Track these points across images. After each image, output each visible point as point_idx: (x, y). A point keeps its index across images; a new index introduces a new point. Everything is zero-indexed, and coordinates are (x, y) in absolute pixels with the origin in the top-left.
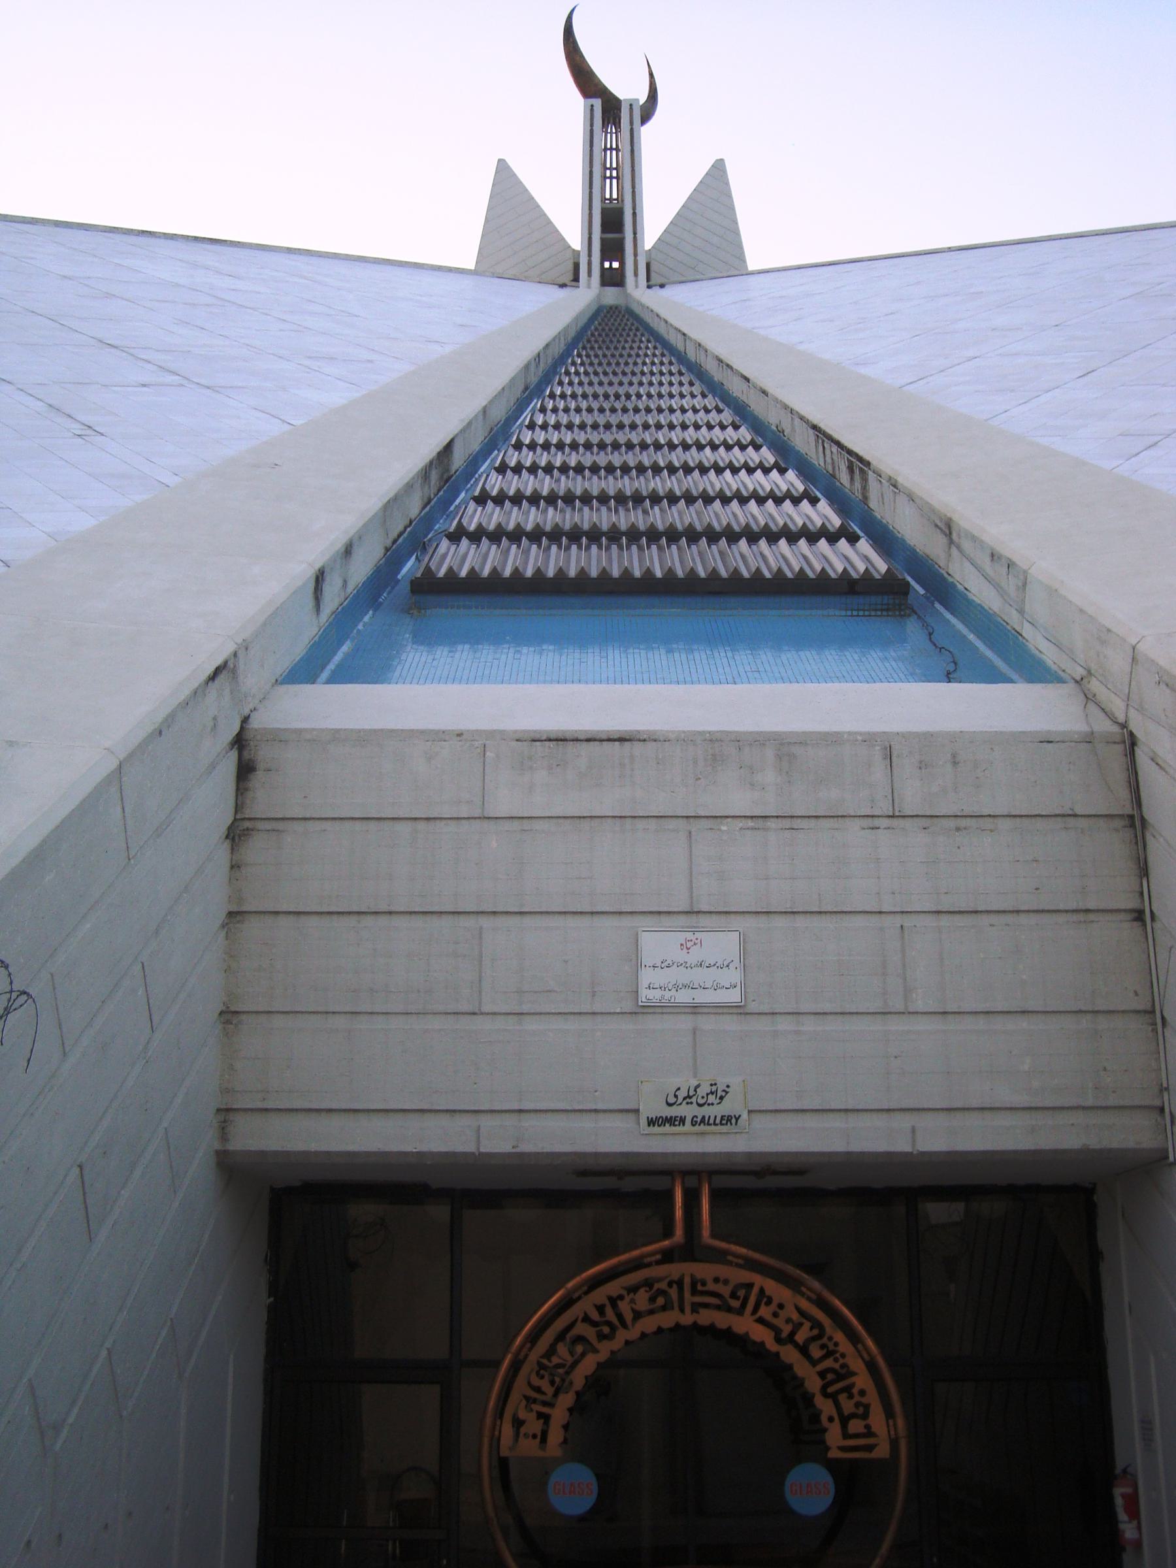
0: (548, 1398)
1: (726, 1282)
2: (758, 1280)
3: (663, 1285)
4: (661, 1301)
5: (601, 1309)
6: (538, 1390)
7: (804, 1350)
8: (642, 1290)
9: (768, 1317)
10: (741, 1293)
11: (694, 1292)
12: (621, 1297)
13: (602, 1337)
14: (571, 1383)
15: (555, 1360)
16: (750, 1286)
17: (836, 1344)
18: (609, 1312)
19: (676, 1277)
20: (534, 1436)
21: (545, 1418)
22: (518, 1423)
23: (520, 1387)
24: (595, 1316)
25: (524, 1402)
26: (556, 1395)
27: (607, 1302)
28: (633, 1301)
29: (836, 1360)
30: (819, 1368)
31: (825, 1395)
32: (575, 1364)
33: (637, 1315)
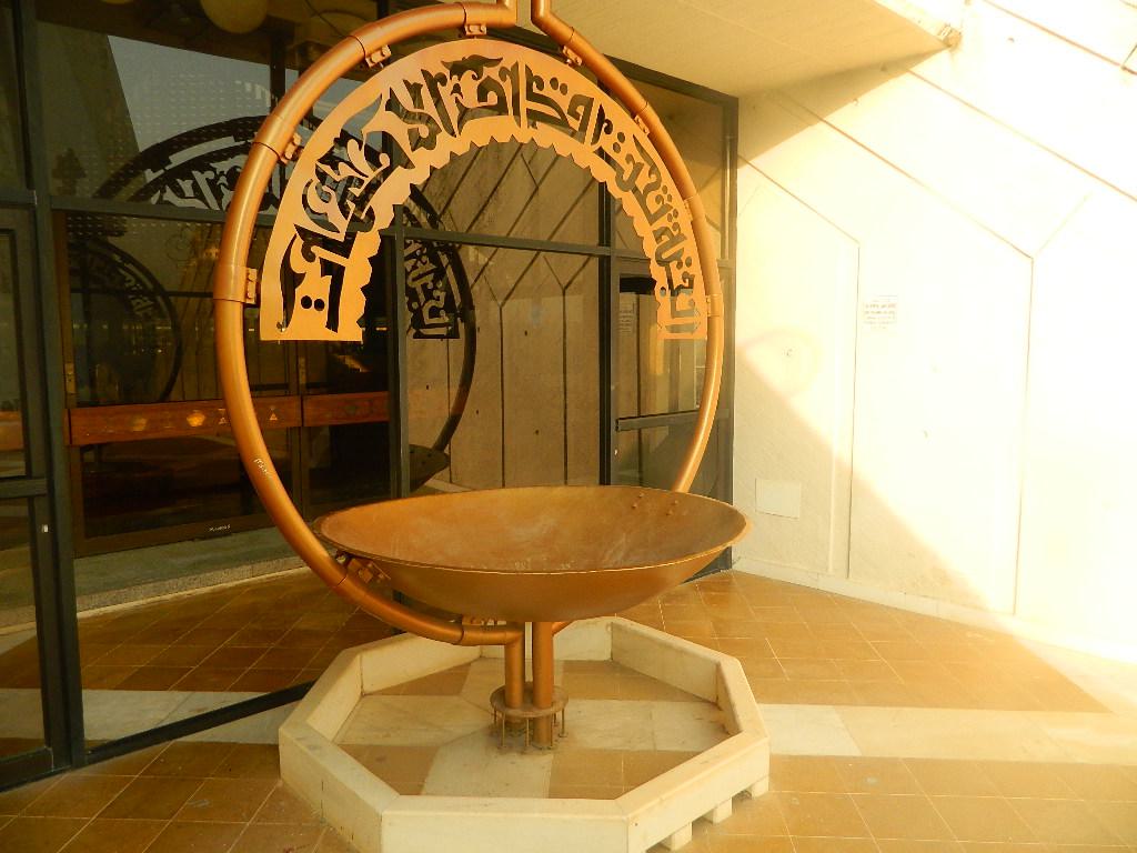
0: (340, 237)
1: (564, 89)
2: (601, 99)
3: (491, 72)
4: (492, 98)
5: (414, 89)
6: (321, 220)
7: (642, 200)
8: (468, 74)
9: (609, 150)
10: (581, 110)
11: (531, 96)
12: (443, 80)
13: (417, 142)
14: (371, 214)
15: (345, 171)
16: (589, 103)
17: (670, 198)
18: (425, 93)
19: (508, 64)
20: (319, 305)
21: (335, 273)
22: (290, 280)
23: (290, 217)
24: (405, 99)
25: (299, 242)
26: (351, 237)
27: (422, 81)
28: (457, 89)
29: (670, 219)
30: (658, 225)
31: (661, 262)
32: (373, 187)
33: (465, 114)
